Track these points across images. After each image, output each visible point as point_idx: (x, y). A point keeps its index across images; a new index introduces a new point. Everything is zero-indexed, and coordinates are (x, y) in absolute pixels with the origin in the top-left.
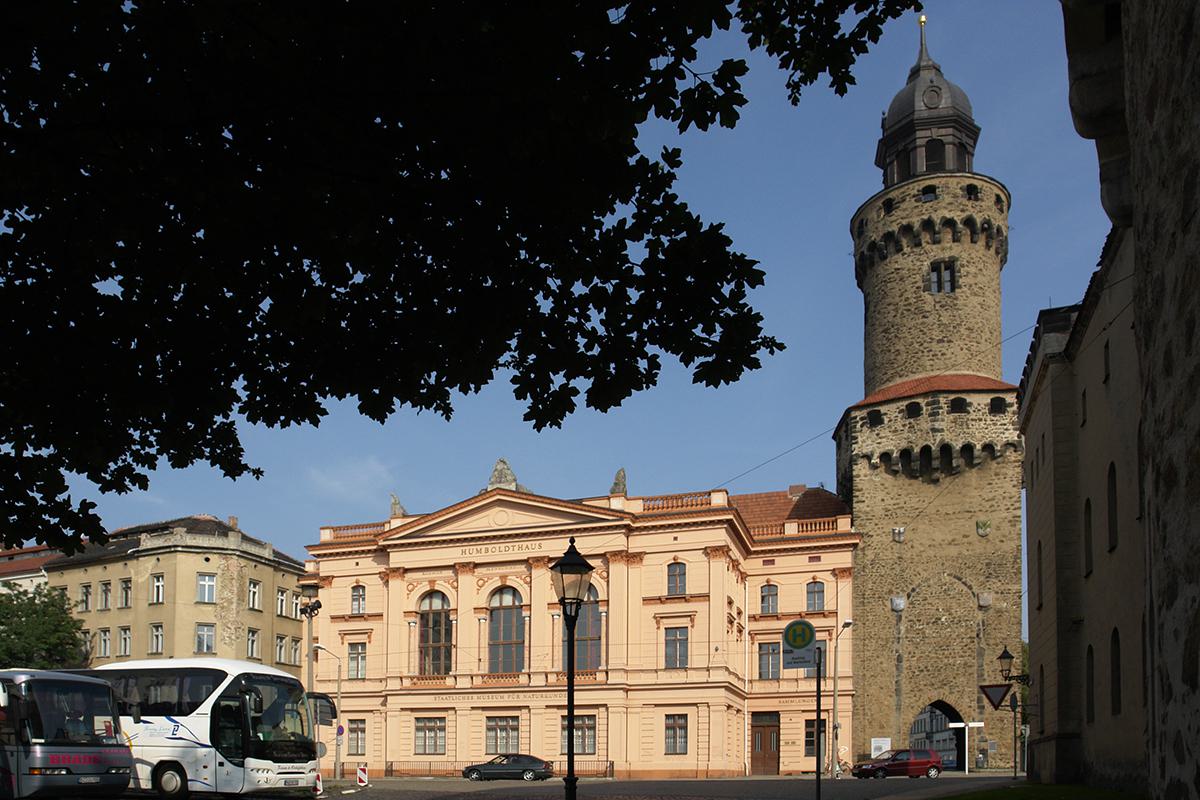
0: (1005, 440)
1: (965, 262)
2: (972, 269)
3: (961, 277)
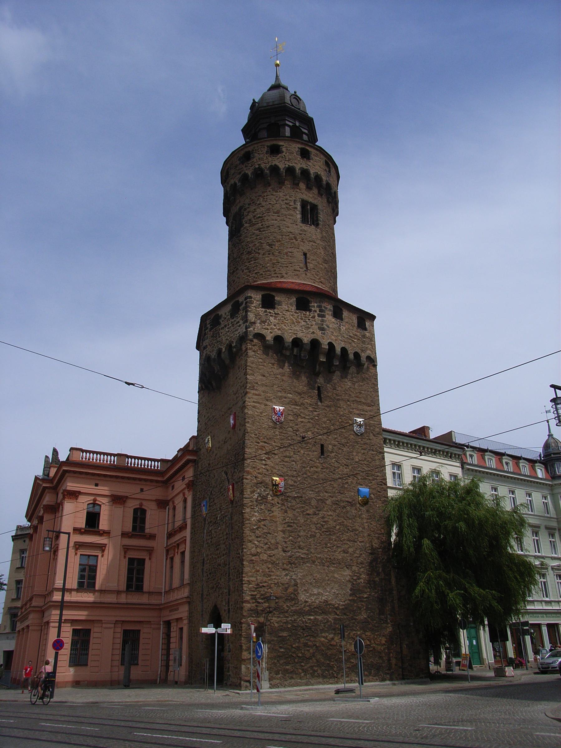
0: (238, 335)
1: (247, 206)
2: (252, 208)
3: (244, 218)
